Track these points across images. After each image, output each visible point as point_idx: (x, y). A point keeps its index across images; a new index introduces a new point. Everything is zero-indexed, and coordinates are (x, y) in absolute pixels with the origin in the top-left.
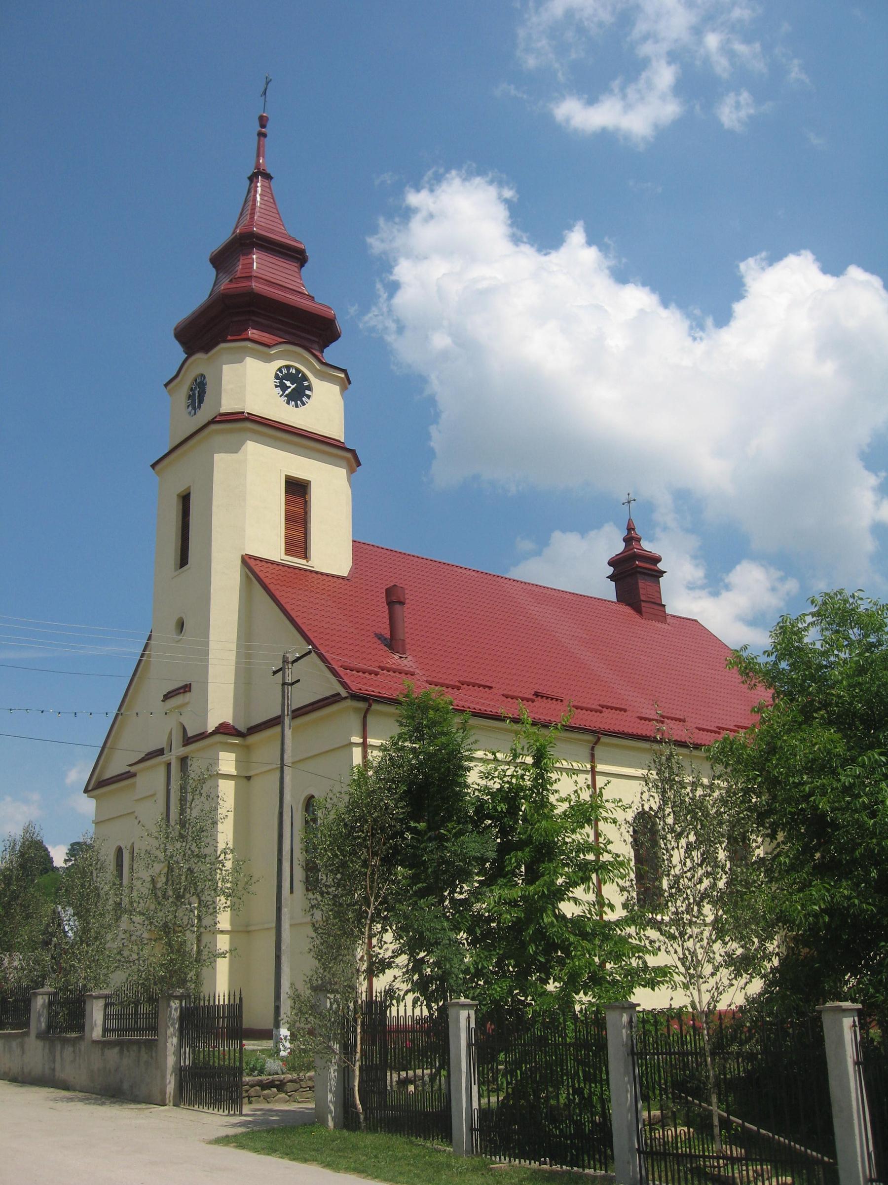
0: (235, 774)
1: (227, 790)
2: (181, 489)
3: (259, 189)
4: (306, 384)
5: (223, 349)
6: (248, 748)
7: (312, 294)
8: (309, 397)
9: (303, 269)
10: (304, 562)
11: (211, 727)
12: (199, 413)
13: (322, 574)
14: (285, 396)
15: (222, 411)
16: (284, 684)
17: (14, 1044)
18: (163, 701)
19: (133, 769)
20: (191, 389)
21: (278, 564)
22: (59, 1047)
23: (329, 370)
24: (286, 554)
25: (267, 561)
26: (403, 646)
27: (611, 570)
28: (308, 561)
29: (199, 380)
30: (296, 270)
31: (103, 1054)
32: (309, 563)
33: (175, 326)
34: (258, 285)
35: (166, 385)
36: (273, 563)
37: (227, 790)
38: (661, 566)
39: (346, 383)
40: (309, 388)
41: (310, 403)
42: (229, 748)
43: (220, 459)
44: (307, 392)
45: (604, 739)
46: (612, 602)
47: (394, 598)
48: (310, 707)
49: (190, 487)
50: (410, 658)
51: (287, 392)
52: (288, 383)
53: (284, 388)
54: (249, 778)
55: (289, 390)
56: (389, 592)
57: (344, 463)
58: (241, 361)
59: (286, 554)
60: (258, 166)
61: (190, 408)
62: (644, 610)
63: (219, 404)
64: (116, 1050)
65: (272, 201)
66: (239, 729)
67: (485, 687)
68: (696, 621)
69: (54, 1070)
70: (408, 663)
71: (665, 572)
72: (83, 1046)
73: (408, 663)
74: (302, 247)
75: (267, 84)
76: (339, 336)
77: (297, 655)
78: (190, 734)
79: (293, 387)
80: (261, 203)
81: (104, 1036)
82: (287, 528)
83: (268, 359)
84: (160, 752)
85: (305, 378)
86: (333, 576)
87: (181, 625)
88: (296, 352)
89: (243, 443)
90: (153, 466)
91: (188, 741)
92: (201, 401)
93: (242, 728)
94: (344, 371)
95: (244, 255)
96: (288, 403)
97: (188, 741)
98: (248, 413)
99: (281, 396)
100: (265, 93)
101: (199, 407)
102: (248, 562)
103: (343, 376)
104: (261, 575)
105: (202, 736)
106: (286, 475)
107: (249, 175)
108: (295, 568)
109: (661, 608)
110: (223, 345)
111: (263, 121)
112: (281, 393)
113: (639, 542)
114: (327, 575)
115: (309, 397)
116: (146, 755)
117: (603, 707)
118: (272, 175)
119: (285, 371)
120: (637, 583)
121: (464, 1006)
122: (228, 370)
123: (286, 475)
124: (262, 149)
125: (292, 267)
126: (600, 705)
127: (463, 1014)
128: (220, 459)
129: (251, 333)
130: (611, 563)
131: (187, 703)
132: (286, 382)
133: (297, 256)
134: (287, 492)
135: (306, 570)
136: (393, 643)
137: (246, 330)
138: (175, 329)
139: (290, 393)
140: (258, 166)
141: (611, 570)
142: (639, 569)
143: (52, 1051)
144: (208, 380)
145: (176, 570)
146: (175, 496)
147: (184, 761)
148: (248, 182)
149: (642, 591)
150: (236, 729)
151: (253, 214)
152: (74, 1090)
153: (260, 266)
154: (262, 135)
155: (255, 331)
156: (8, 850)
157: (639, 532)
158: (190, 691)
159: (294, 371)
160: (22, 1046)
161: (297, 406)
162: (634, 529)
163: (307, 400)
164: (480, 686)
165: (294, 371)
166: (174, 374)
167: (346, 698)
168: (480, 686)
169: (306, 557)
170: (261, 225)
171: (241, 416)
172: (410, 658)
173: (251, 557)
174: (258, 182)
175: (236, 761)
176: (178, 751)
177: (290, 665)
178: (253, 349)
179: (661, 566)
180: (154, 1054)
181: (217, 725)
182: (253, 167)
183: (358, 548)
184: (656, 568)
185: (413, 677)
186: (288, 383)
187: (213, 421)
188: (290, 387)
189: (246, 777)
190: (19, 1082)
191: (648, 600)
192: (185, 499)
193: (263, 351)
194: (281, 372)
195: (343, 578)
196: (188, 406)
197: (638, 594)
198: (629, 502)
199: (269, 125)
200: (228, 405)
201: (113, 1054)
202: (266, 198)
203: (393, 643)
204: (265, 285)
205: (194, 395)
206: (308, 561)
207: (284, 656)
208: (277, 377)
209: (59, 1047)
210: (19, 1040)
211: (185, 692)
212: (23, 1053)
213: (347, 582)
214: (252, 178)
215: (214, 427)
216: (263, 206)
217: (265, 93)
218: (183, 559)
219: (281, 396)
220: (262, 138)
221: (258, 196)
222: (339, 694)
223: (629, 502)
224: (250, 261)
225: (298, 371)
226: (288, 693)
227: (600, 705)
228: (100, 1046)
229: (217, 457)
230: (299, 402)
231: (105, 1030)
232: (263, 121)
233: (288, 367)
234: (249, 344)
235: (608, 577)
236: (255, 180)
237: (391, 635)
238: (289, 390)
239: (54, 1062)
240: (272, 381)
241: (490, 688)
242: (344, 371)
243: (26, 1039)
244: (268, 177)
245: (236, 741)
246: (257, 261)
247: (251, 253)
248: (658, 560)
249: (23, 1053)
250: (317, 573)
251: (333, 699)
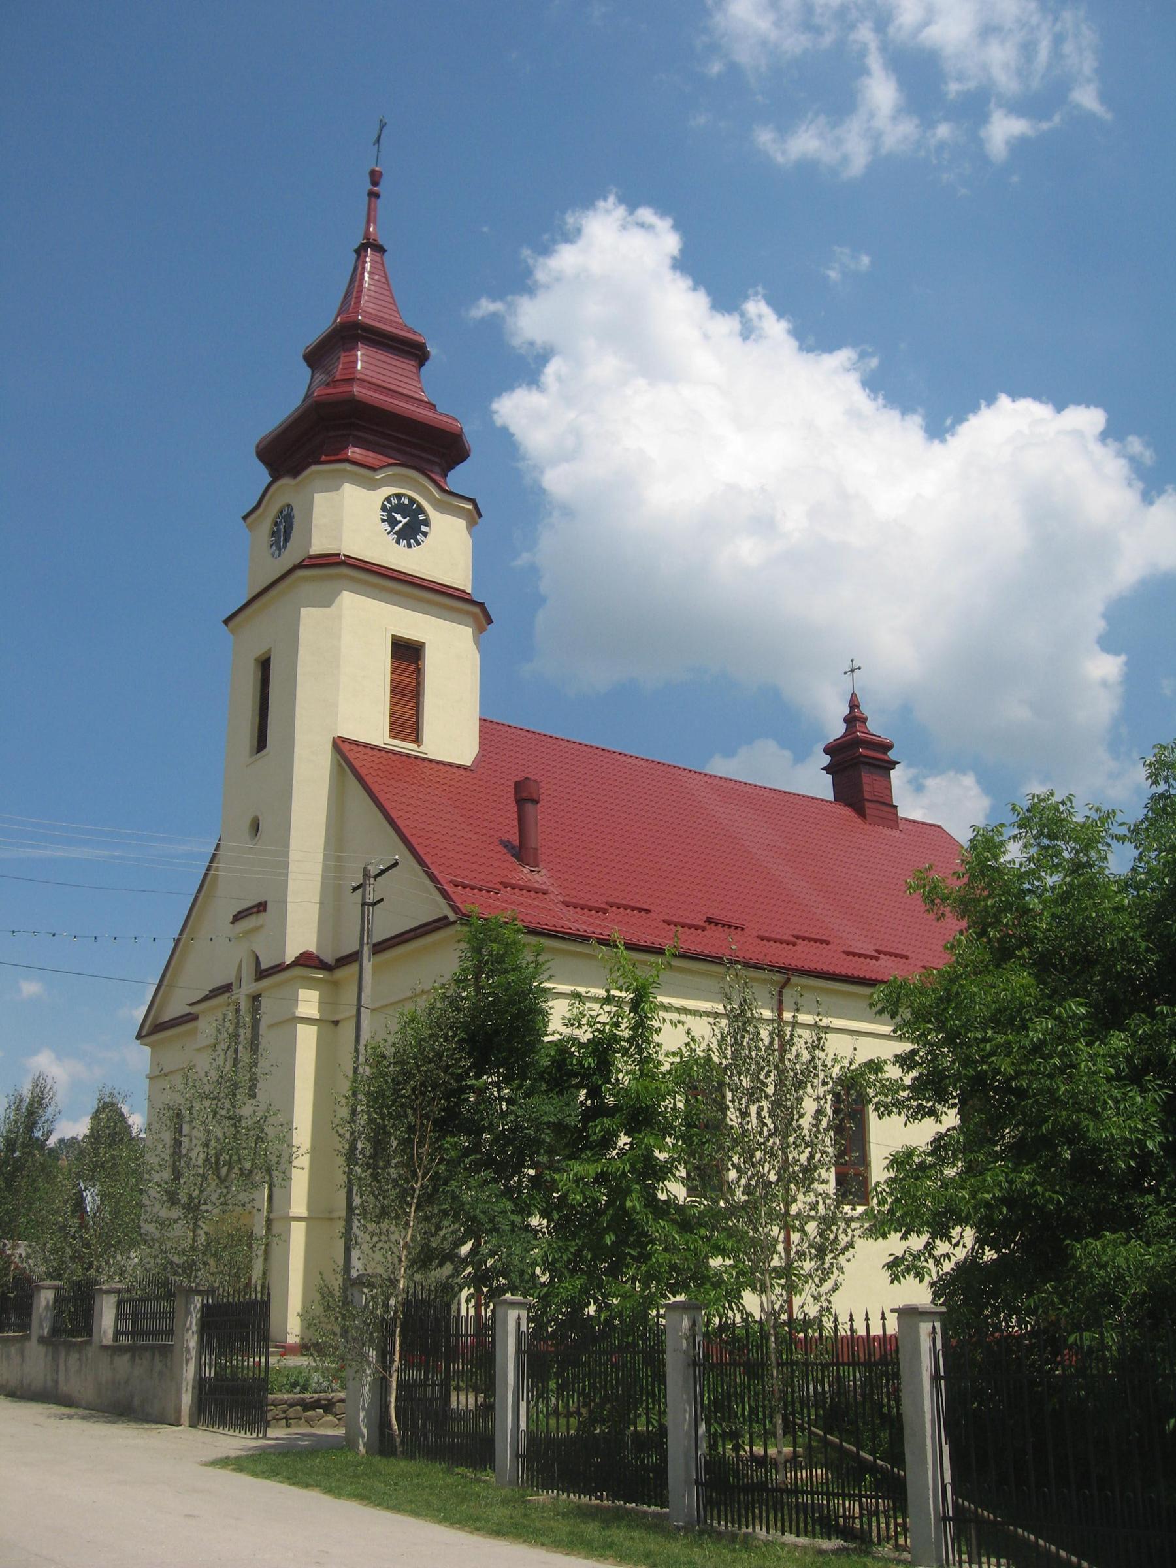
0: (318, 1017)
1: (307, 1039)
2: (259, 651)
3: (368, 266)
4: (422, 517)
5: (318, 472)
6: (336, 984)
7: (433, 403)
8: (425, 534)
9: (423, 368)
10: (414, 746)
11: (290, 957)
12: (285, 553)
13: (437, 762)
14: (395, 534)
15: (311, 553)
16: (364, 904)
17: (13, 1350)
18: (232, 923)
19: (194, 1010)
20: (276, 524)
21: (380, 749)
22: (63, 1354)
23: (452, 501)
24: (391, 737)
25: (366, 746)
26: (536, 855)
27: (826, 760)
28: (419, 746)
29: (285, 513)
30: (414, 370)
31: (112, 1363)
32: (421, 749)
33: (256, 441)
34: (361, 390)
35: (245, 518)
36: (373, 748)
37: (307, 1039)
38: (892, 755)
39: (474, 515)
40: (426, 523)
41: (427, 542)
42: (311, 984)
43: (309, 616)
44: (424, 528)
46: (827, 801)
47: (525, 795)
48: (413, 933)
49: (270, 650)
50: (543, 872)
51: (397, 528)
52: (399, 517)
53: (392, 522)
54: (336, 1023)
55: (400, 525)
56: (518, 786)
57: (470, 620)
58: (337, 488)
59: (391, 737)
60: (367, 234)
61: (274, 548)
62: (868, 811)
63: (309, 545)
64: (127, 1357)
65: (384, 280)
66: (326, 960)
67: (640, 910)
68: (939, 827)
69: (56, 1382)
70: (540, 878)
71: (898, 763)
72: (90, 1352)
73: (540, 878)
74: (422, 340)
75: (382, 128)
76: (468, 456)
77: (381, 867)
78: (264, 966)
79: (405, 521)
80: (369, 284)
81: (115, 1340)
82: (392, 703)
83: (373, 485)
84: (226, 988)
85: (421, 510)
86: (452, 765)
87: (256, 826)
88: (408, 477)
89: (337, 594)
90: (226, 622)
91: (261, 974)
92: (287, 540)
93: (329, 958)
94: (472, 501)
95: (345, 352)
96: (398, 542)
97: (261, 974)
98: (345, 555)
99: (389, 533)
100: (378, 141)
101: (285, 546)
102: (341, 746)
103: (470, 507)
104: (357, 764)
105: (279, 968)
107: (356, 247)
108: (402, 754)
109: (892, 810)
110: (314, 468)
112: (389, 529)
113: (865, 723)
114: (444, 764)
115: (425, 534)
116: (211, 991)
117: (798, 937)
118: (386, 247)
119: (394, 501)
120: (860, 776)
121: (513, 1304)
122: (322, 502)
124: (373, 213)
125: (408, 365)
126: (794, 936)
127: (512, 1314)
128: (309, 616)
129: (353, 452)
130: (827, 751)
131: (261, 927)
132: (396, 515)
133: (416, 353)
134: (393, 657)
135: (416, 758)
136: (522, 852)
137: (346, 448)
138: (257, 447)
139: (400, 529)
140: (367, 234)
141: (826, 760)
142: (863, 759)
143: (55, 1359)
144: (296, 512)
145: (251, 755)
146: (253, 661)
147: (256, 998)
148: (355, 256)
149: (866, 787)
150: (321, 961)
151: (359, 297)
152: (77, 1406)
153: (365, 364)
154: (373, 195)
155: (357, 450)
156: (13, 1108)
157: (866, 709)
158: (265, 910)
159: (406, 502)
160: (22, 1353)
161: (409, 546)
162: (858, 707)
163: (423, 538)
164: (633, 909)
165: (406, 502)
166: (255, 504)
167: (454, 922)
168: (633, 909)
169: (417, 739)
170: (369, 310)
171: (336, 560)
172: (543, 872)
173: (345, 740)
174: (366, 256)
175: (320, 1002)
176: (249, 987)
177: (372, 880)
179: (892, 755)
180: (169, 1364)
181: (297, 954)
182: (362, 238)
183: (488, 729)
184: (886, 757)
185: (545, 896)
186: (399, 517)
187: (299, 566)
188: (400, 522)
189: (333, 1022)
190: (18, 1397)
191: (875, 799)
192: (265, 665)
193: (366, 474)
194: (390, 502)
195: (465, 768)
196: (272, 545)
197: (861, 791)
198: (852, 671)
199: (384, 182)
200: (319, 545)
201: (123, 1361)
202: (376, 277)
203: (522, 852)
204: (375, 391)
205: (279, 530)
206: (419, 746)
207: (365, 869)
208: (384, 508)
209: (63, 1354)
210: (18, 1345)
211: (259, 912)
212: (23, 1361)
213: (469, 773)
214: (360, 251)
215: (301, 573)
216: (372, 288)
217: (378, 141)
218: (261, 743)
219: (389, 533)
220: (373, 199)
221: (366, 276)
222: (446, 917)
223: (852, 671)
224: (352, 359)
225: (412, 500)
226: (368, 915)
227: (794, 936)
228: (110, 1352)
229: (304, 611)
230: (412, 541)
231: (117, 1333)
234: (348, 467)
235: (823, 769)
236: (363, 254)
237: (520, 842)
238: (400, 525)
239: (57, 1373)
240: (377, 514)
241: (648, 911)
242: (472, 501)
243: (27, 1344)
244: (380, 249)
245: (320, 975)
246: (362, 358)
247: (355, 348)
248: (888, 747)
249: (23, 1361)
250: (431, 761)
251: (441, 923)
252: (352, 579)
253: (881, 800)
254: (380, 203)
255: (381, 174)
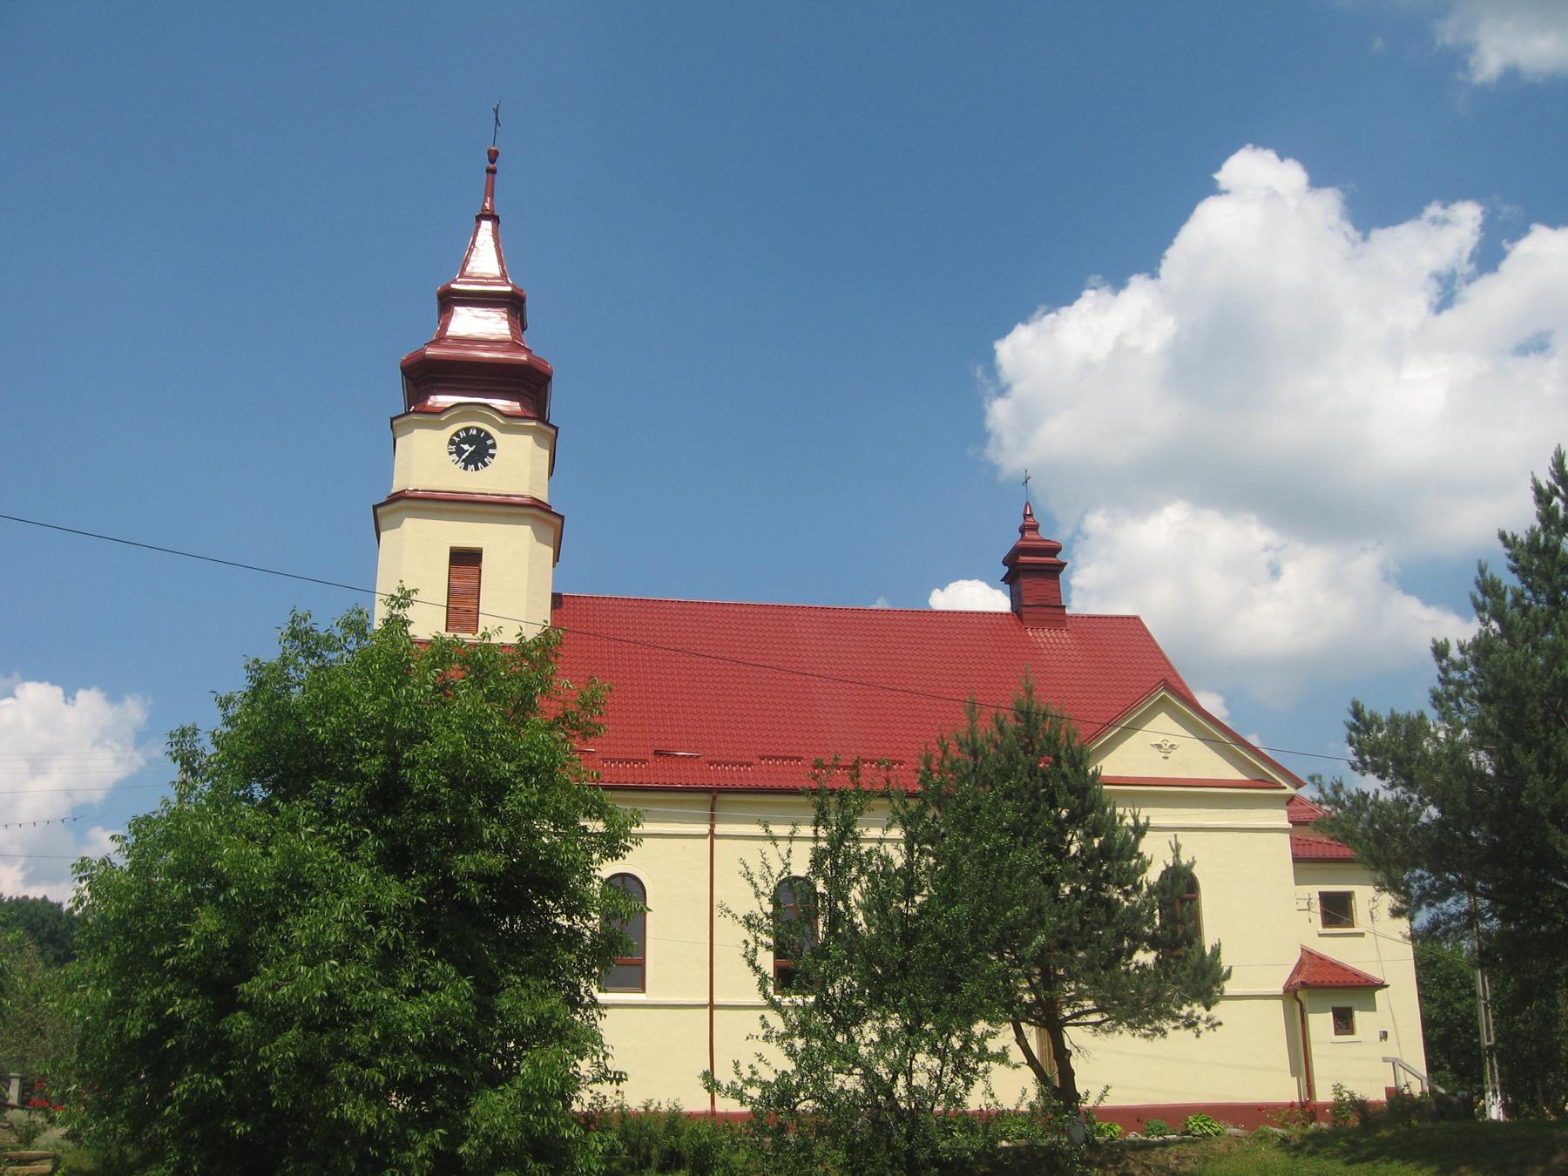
4: (489, 442)
8: (492, 456)
40: (494, 446)
41: (494, 464)
44: (491, 451)
45: (722, 797)
51: (464, 457)
52: (466, 447)
53: (460, 452)
55: (467, 454)
60: (484, 209)
62: (1025, 616)
79: (472, 449)
83: (442, 426)
85: (488, 436)
96: (466, 468)
106: (451, 549)
109: (1059, 611)
111: (493, 156)
115: (492, 456)
119: (462, 435)
123: (452, 549)
130: (1005, 563)
140: (484, 209)
141: (1006, 569)
154: (492, 172)
159: (475, 432)
165: (475, 432)
178: (421, 421)
179: (1060, 557)
186: (466, 447)
191: (1037, 603)
208: (452, 442)
225: (479, 430)
230: (480, 464)
232: (493, 156)
233: (467, 430)
238: (467, 454)
248: (1054, 550)
252: (408, 508)
253: (1045, 603)
254: (498, 177)
255: (496, 153)
